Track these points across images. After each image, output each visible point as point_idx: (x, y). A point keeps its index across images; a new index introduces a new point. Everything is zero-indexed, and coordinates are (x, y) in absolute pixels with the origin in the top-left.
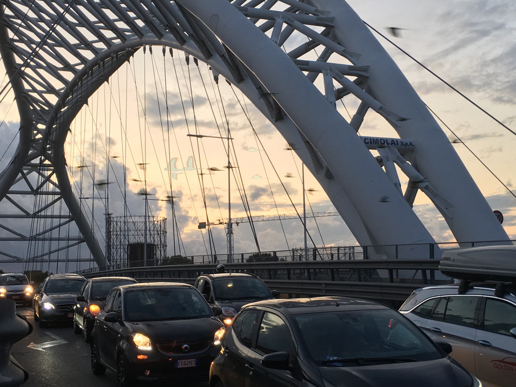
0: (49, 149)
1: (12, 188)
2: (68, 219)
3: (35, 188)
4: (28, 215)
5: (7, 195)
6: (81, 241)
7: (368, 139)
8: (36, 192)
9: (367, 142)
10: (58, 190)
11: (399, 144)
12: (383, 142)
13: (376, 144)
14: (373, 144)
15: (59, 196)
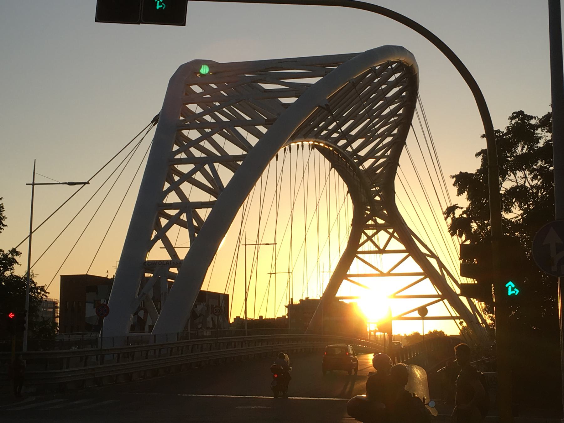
0: (383, 209)
1: (360, 249)
2: (423, 277)
3: (382, 248)
4: (382, 274)
5: (359, 255)
6: (442, 298)
7: (150, 262)
8: (382, 251)
9: (149, 264)
10: (402, 247)
11: (172, 262)
12: (160, 263)
13: (155, 264)
14: (154, 265)
15: (407, 254)
